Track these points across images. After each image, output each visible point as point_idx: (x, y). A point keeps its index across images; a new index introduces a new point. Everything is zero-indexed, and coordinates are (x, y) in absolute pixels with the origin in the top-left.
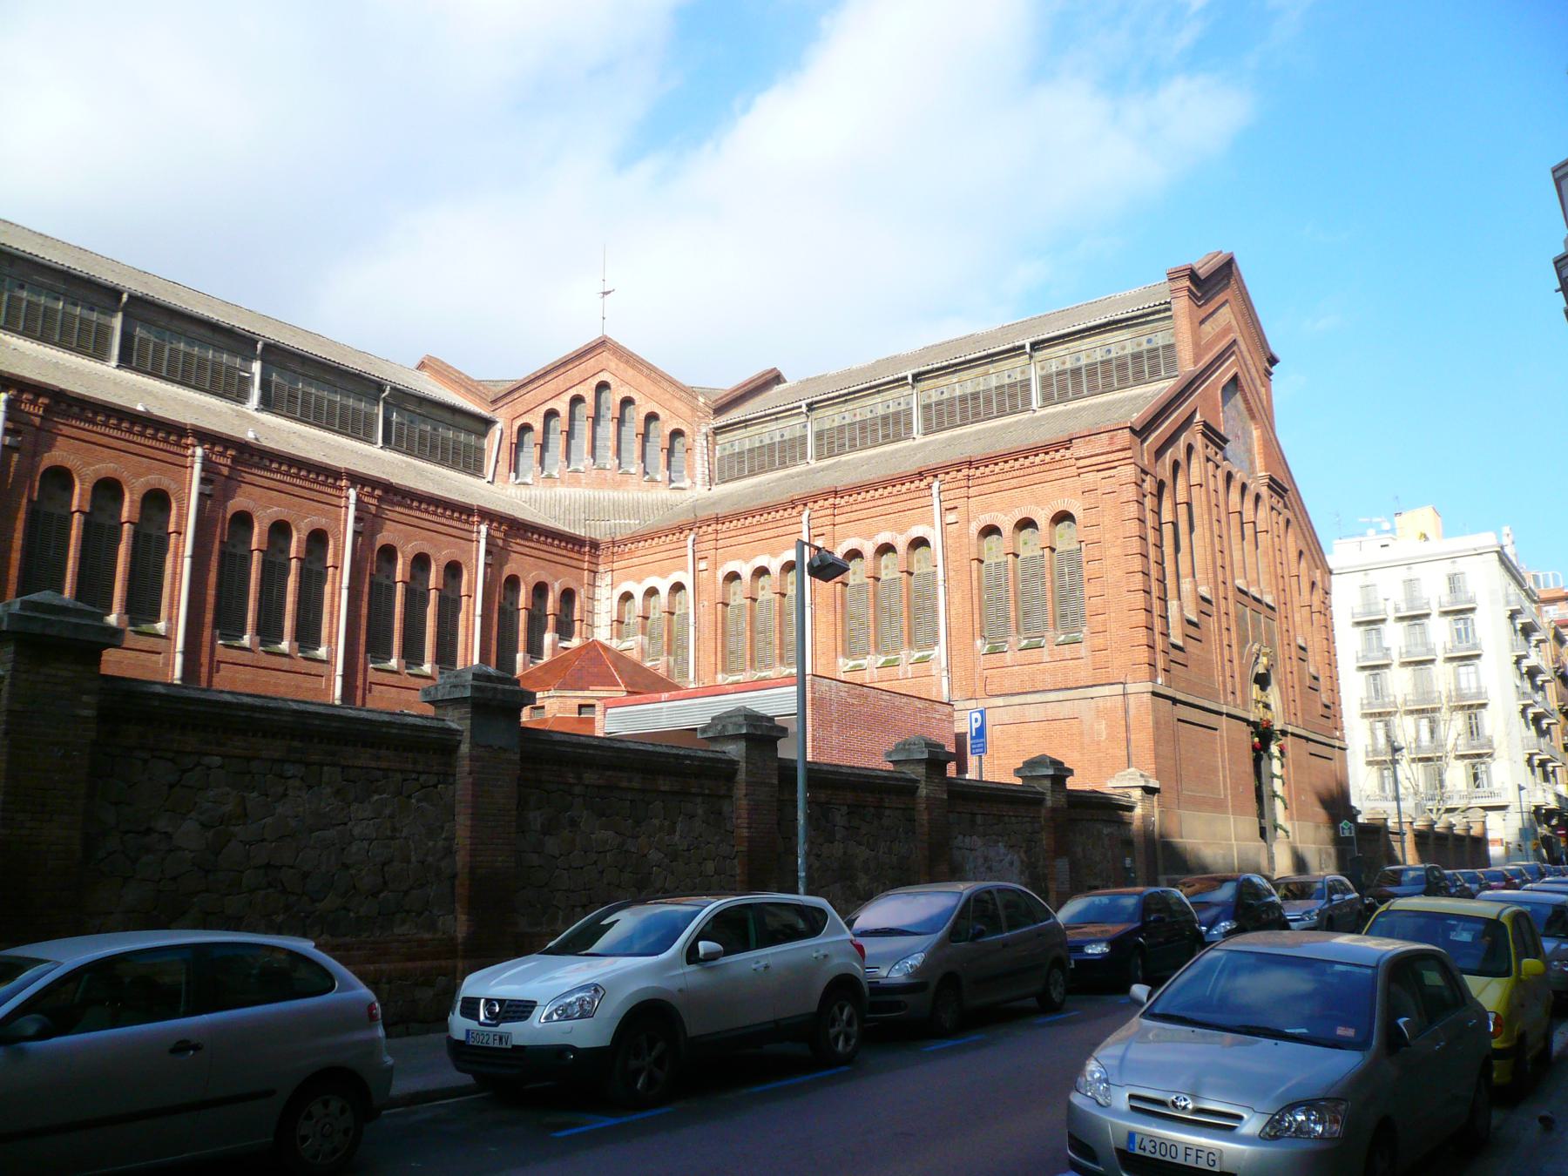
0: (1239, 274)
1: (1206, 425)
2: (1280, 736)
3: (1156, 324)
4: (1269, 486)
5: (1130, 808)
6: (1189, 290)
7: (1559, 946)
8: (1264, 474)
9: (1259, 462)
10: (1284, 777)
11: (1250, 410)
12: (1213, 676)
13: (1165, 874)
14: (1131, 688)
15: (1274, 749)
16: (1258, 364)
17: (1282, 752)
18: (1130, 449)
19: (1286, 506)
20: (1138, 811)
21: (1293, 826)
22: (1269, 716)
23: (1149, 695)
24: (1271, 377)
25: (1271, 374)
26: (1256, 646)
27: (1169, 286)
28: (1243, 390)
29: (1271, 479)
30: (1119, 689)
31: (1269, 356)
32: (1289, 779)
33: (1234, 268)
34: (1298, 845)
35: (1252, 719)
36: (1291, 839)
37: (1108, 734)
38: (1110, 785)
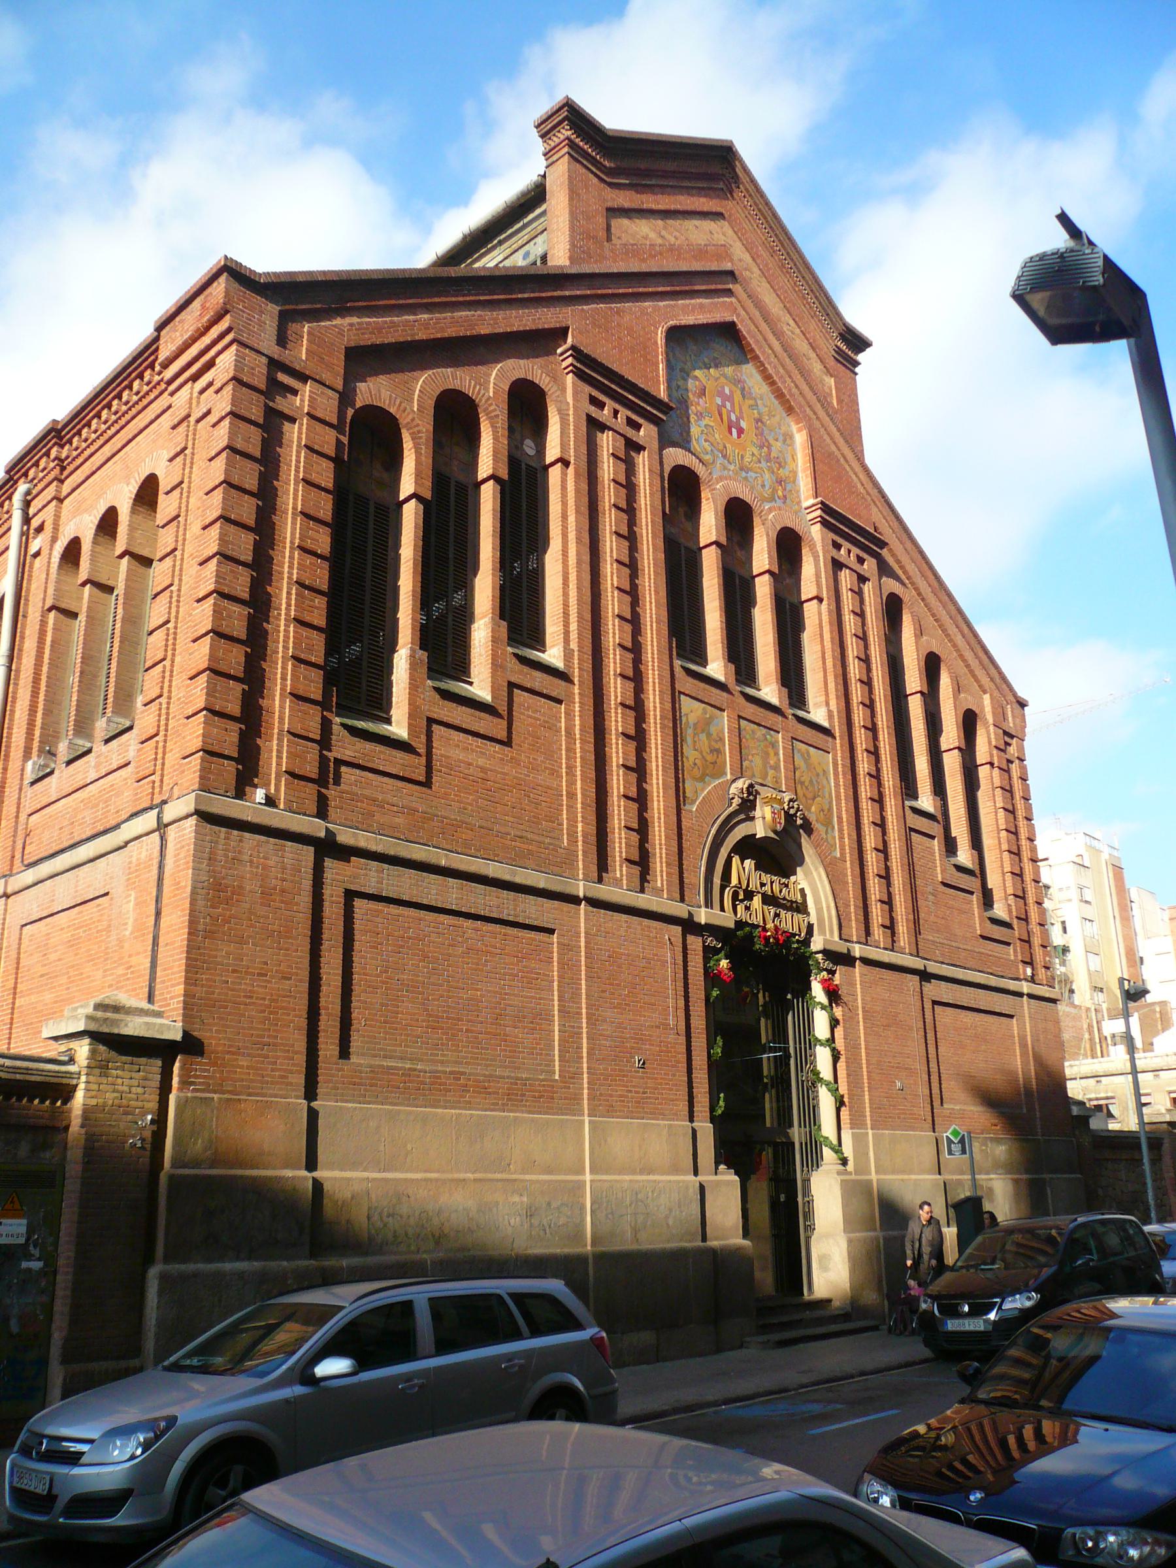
0: (753, 181)
1: (577, 352)
2: (828, 965)
3: (534, 225)
4: (825, 523)
5: (67, 1093)
6: (572, 144)
7: (1142, 1552)
8: (812, 501)
9: (804, 483)
10: (840, 1044)
11: (780, 395)
12: (554, 818)
13: (167, 1259)
14: (170, 813)
15: (818, 991)
16: (821, 342)
17: (833, 995)
18: (227, 312)
19: (884, 569)
20: (79, 1096)
21: (859, 1141)
22: (790, 922)
23: (192, 821)
24: (857, 370)
25: (856, 364)
26: (742, 784)
27: (539, 146)
28: (756, 358)
29: (825, 508)
30: (148, 820)
31: (841, 328)
32: (853, 1046)
33: (739, 170)
34: (874, 1177)
35: (703, 922)
36: (850, 1167)
37: (136, 920)
38: (46, 1033)
